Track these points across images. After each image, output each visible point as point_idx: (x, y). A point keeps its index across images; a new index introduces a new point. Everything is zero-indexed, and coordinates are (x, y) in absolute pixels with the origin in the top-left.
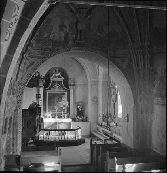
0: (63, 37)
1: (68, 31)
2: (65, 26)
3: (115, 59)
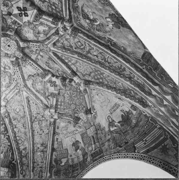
0: (82, 156)
1: (83, 146)
2: (77, 141)
3: (149, 154)
